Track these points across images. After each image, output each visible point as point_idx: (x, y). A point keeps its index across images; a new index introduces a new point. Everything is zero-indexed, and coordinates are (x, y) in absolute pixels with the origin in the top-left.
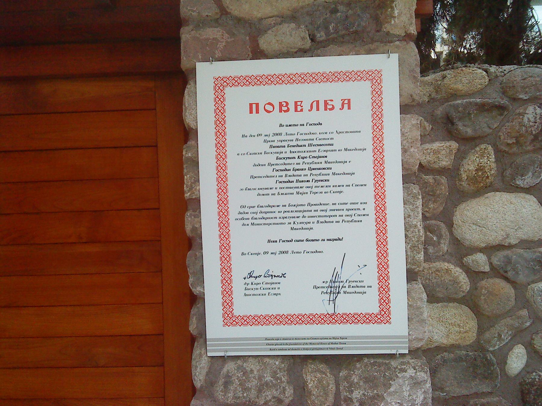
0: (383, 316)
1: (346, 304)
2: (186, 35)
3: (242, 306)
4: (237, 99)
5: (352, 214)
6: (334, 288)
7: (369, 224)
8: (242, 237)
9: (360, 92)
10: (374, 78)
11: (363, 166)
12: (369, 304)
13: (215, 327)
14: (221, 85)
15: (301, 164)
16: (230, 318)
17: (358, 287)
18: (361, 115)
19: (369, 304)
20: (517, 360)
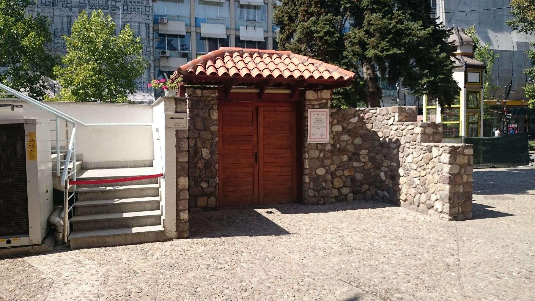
0: (326, 138)
1: (323, 137)
2: (307, 106)
3: (312, 137)
4: (312, 113)
5: (324, 127)
6: (321, 135)
7: (325, 129)
8: (312, 129)
9: (325, 113)
10: (327, 112)
11: (325, 122)
12: (325, 137)
13: (308, 140)
14: (311, 112)
15: (319, 121)
16: (310, 139)
17: (324, 135)
18: (325, 116)
19: (325, 137)
20: (338, 146)
